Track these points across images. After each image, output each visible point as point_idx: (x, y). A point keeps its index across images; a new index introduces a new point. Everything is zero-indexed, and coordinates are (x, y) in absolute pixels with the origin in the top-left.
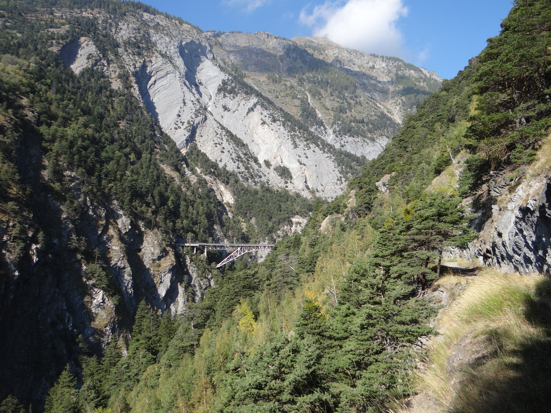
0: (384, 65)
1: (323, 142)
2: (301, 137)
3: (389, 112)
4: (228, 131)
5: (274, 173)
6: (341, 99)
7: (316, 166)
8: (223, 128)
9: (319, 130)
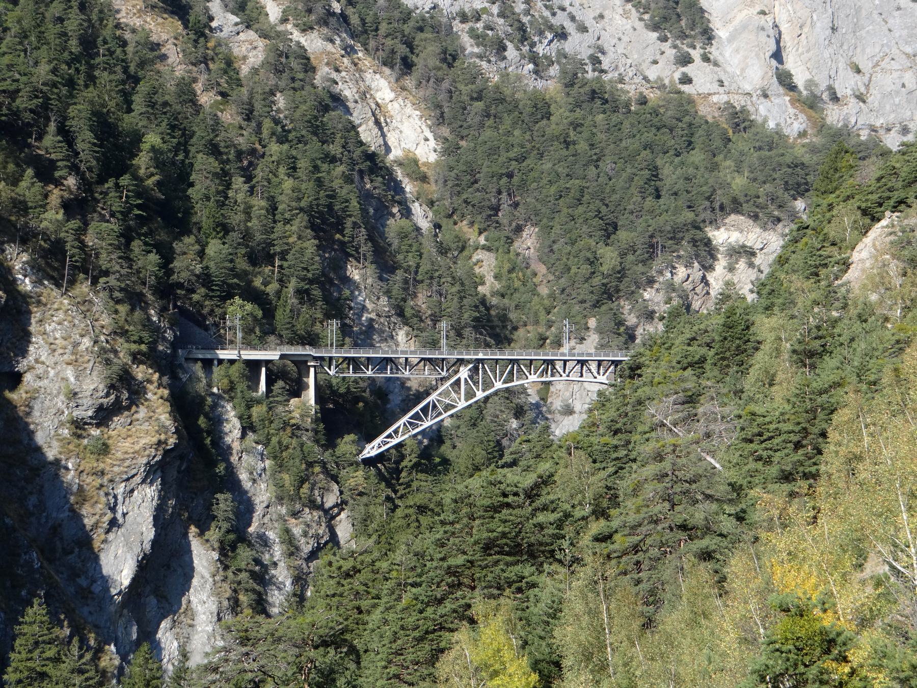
5: (626, 15)
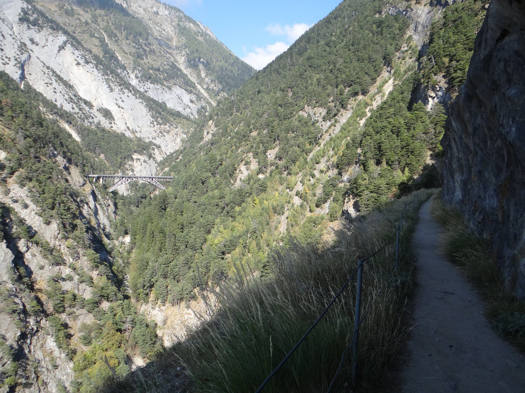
0: (167, 13)
1: (133, 87)
2: (115, 81)
3: (175, 61)
4: (54, 72)
6: (137, 44)
7: (132, 109)
8: (48, 68)
9: (123, 74)
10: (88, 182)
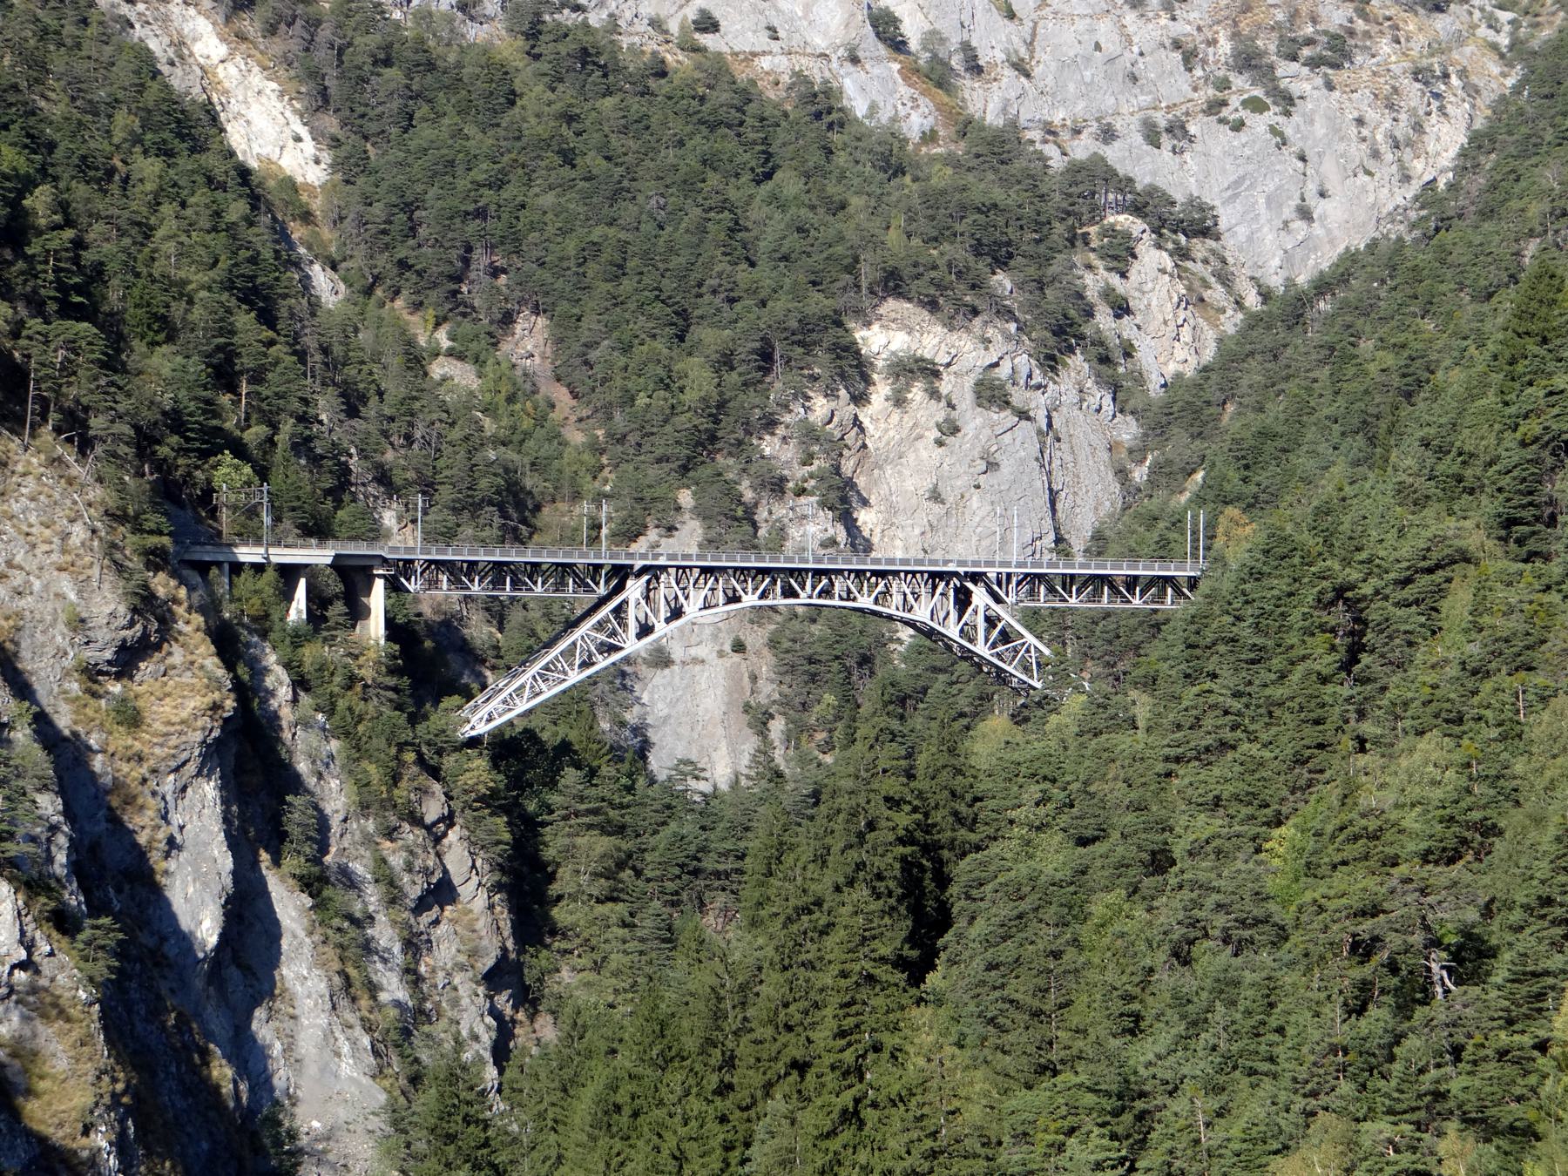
10: (190, 624)
